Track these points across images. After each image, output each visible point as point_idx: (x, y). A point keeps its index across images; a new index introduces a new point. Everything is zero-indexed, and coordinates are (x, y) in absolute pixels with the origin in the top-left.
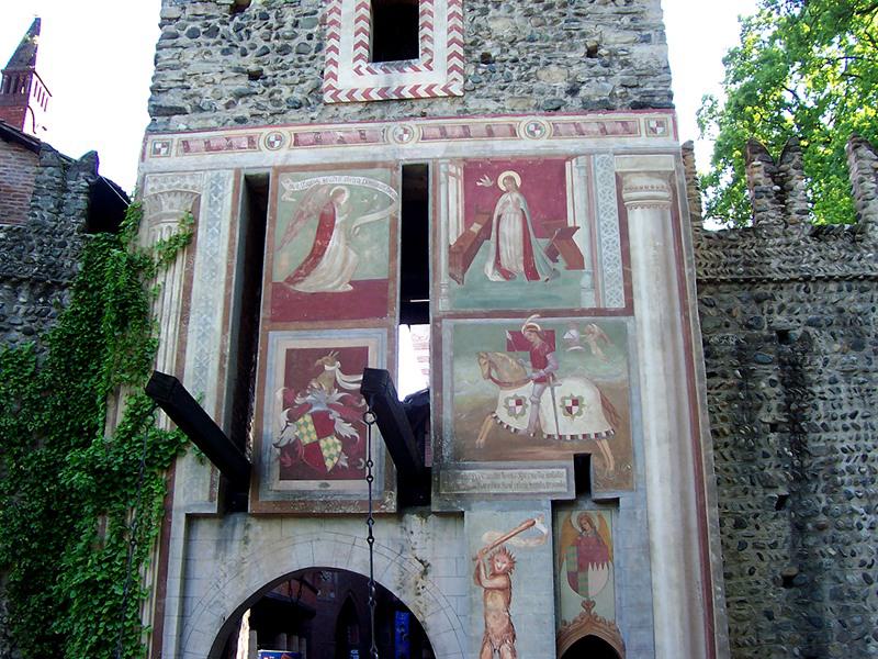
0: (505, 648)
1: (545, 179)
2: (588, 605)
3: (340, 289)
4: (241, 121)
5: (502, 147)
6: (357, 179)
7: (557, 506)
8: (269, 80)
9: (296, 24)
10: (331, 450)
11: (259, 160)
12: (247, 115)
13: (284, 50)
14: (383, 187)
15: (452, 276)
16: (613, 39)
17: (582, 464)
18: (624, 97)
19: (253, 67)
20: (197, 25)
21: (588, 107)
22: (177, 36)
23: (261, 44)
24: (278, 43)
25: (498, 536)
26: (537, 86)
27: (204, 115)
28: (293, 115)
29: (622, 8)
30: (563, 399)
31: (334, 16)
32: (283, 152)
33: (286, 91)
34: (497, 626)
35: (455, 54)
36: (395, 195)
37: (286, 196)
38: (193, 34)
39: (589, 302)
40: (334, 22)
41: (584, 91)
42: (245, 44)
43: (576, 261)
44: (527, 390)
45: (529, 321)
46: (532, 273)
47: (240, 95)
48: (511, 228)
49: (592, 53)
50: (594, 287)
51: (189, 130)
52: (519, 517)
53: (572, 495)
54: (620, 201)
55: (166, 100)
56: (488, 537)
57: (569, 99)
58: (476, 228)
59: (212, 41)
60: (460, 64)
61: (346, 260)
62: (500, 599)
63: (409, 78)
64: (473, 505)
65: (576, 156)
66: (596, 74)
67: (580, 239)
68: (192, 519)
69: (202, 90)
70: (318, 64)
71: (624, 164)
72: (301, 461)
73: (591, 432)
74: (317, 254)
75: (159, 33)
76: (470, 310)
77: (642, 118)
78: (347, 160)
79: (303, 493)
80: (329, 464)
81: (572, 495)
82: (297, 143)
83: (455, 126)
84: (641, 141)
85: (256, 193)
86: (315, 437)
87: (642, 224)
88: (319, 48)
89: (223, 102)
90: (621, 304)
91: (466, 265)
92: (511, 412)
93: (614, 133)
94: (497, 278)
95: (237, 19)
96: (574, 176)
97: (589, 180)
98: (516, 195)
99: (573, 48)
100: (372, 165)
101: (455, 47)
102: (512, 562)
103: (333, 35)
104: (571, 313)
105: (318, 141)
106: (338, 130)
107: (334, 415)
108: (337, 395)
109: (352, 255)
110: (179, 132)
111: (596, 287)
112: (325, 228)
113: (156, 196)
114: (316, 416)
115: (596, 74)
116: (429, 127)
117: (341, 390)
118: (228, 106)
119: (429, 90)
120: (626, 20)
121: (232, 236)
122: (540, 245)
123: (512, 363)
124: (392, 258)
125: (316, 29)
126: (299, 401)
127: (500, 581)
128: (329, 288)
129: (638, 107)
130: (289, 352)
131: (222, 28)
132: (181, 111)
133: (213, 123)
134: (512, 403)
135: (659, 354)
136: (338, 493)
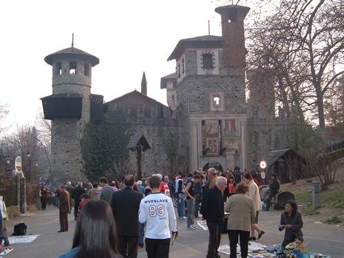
1: (233, 121)
5: (228, 118)
10: (214, 151)
11: (204, 118)
21: (238, 113)
37: (207, 122)
48: (230, 127)
74: (210, 130)
85: (203, 122)
87: (242, 127)
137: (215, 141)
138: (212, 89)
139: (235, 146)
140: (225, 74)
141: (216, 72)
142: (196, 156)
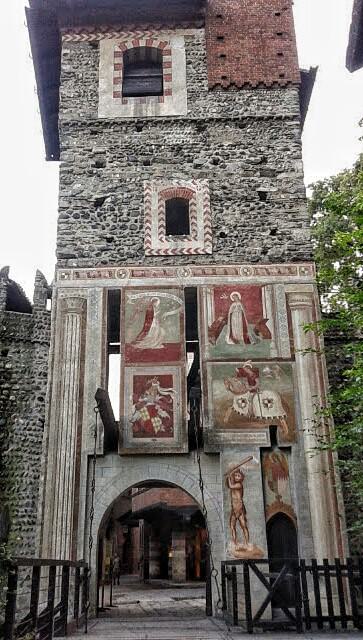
0: (241, 517)
2: (279, 497)
3: (158, 347)
4: (104, 263)
5: (231, 279)
6: (164, 294)
7: (263, 450)
8: (117, 243)
9: (128, 215)
10: (157, 423)
12: (107, 259)
13: (123, 227)
14: (175, 298)
15: (210, 341)
16: (283, 226)
17: (273, 430)
18: (289, 255)
19: (109, 236)
20: (78, 212)
21: (272, 260)
22: (68, 217)
23: (112, 224)
24: (121, 224)
25: (236, 464)
26: (247, 250)
27: (87, 259)
28: (130, 261)
29: (288, 210)
30: (263, 400)
31: (148, 211)
32: (127, 280)
33: (126, 248)
34: (237, 506)
35: (208, 233)
36: (181, 302)
38: (76, 217)
39: (274, 354)
40: (147, 214)
41: (270, 252)
42: (102, 223)
43: (268, 336)
44: (246, 396)
45: (246, 363)
46: (247, 341)
47: (103, 250)
48: (236, 320)
49: (273, 232)
50: (277, 347)
51: (78, 267)
52: (245, 455)
53: (269, 445)
54: (288, 306)
55: (65, 251)
56: (231, 465)
57: (262, 256)
58: (221, 319)
59: (87, 221)
60: (211, 238)
61: (160, 332)
62: (238, 494)
63: (188, 245)
64: (225, 449)
65: (267, 284)
66: (276, 244)
67: (269, 324)
68: (90, 457)
69: (83, 246)
70: (141, 235)
71: (290, 289)
72: (143, 429)
73: (277, 415)
74: (146, 329)
75: (57, 215)
76: (219, 358)
77: (298, 265)
78: (157, 284)
79: (145, 444)
80: (156, 431)
81: (269, 445)
82: (133, 276)
83: (208, 269)
84: (297, 278)
85: (114, 300)
86: (149, 417)
88: (141, 227)
89: (95, 253)
90: (290, 356)
91: (217, 336)
92: (240, 406)
93: (284, 274)
94: (232, 343)
95: (98, 210)
96: (266, 294)
97: (272, 296)
98: (239, 304)
99: (264, 231)
100: (170, 287)
101: (207, 229)
102: (243, 476)
103: (147, 221)
104: (267, 360)
105: (143, 275)
106: (153, 269)
107: (157, 407)
108: (159, 398)
109: (163, 332)
110: (73, 267)
111: (278, 348)
112: (149, 317)
113: (64, 300)
114: (149, 408)
115: (276, 244)
116: (198, 269)
117: (160, 395)
118: (97, 255)
119: (196, 250)
120: (290, 216)
121: (104, 321)
122: (251, 327)
123: (238, 383)
124: (182, 330)
125: (139, 217)
126: (140, 400)
127: (237, 485)
128: (153, 346)
129: (295, 260)
130: (135, 377)
131: (91, 214)
132: (74, 257)
133: (90, 264)
134: (240, 402)
135: (307, 379)
136: (161, 443)
137: (166, 381)
138: (157, 168)
139: (265, 404)
140: (214, 112)
141: (173, 105)
142: (66, 455)
